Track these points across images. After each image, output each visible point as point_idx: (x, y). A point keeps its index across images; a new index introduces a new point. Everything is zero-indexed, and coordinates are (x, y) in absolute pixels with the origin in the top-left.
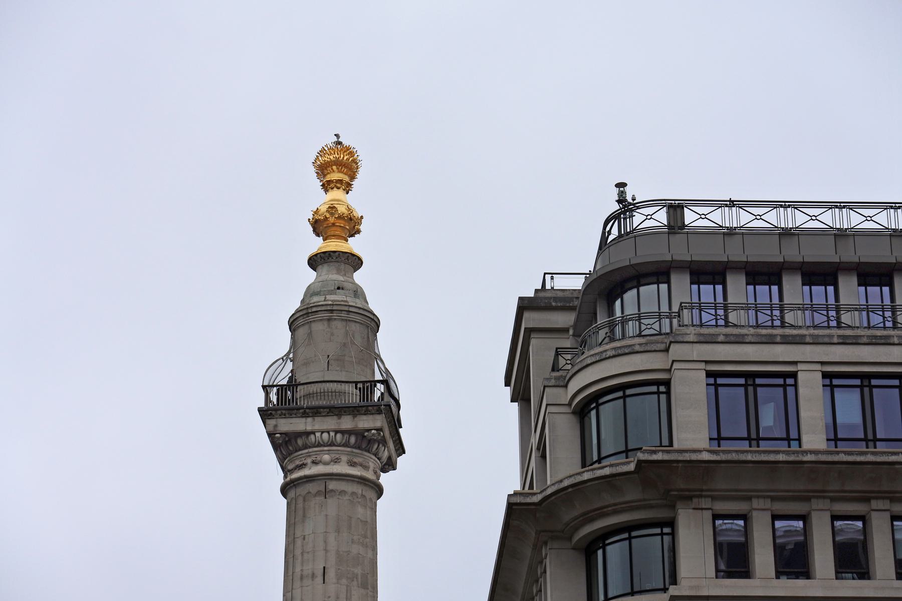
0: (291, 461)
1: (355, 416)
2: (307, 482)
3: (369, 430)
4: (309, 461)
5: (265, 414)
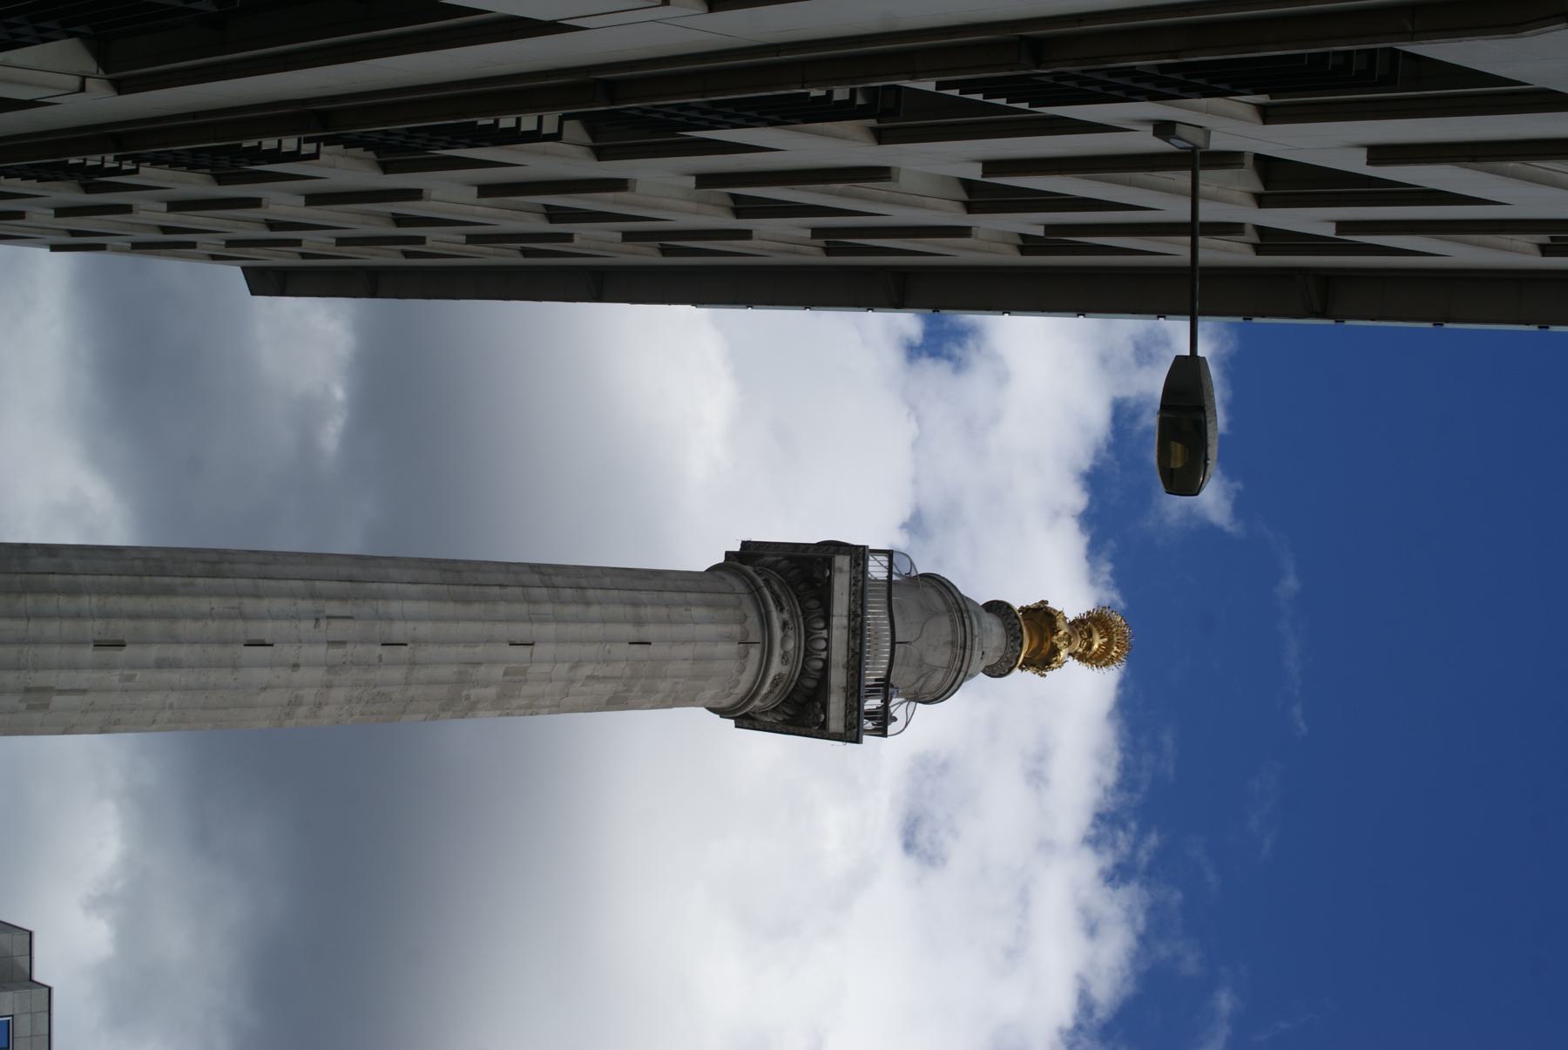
0: (781, 584)
1: (846, 689)
2: (760, 614)
3: (825, 708)
4: (786, 616)
5: (859, 555)
